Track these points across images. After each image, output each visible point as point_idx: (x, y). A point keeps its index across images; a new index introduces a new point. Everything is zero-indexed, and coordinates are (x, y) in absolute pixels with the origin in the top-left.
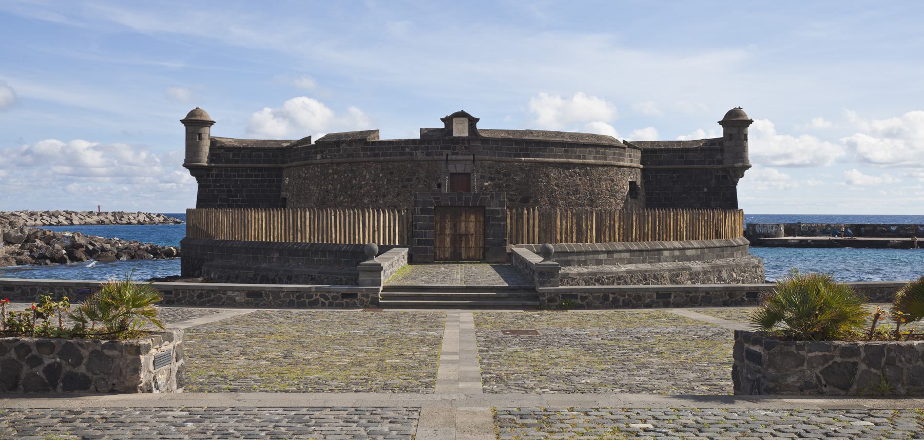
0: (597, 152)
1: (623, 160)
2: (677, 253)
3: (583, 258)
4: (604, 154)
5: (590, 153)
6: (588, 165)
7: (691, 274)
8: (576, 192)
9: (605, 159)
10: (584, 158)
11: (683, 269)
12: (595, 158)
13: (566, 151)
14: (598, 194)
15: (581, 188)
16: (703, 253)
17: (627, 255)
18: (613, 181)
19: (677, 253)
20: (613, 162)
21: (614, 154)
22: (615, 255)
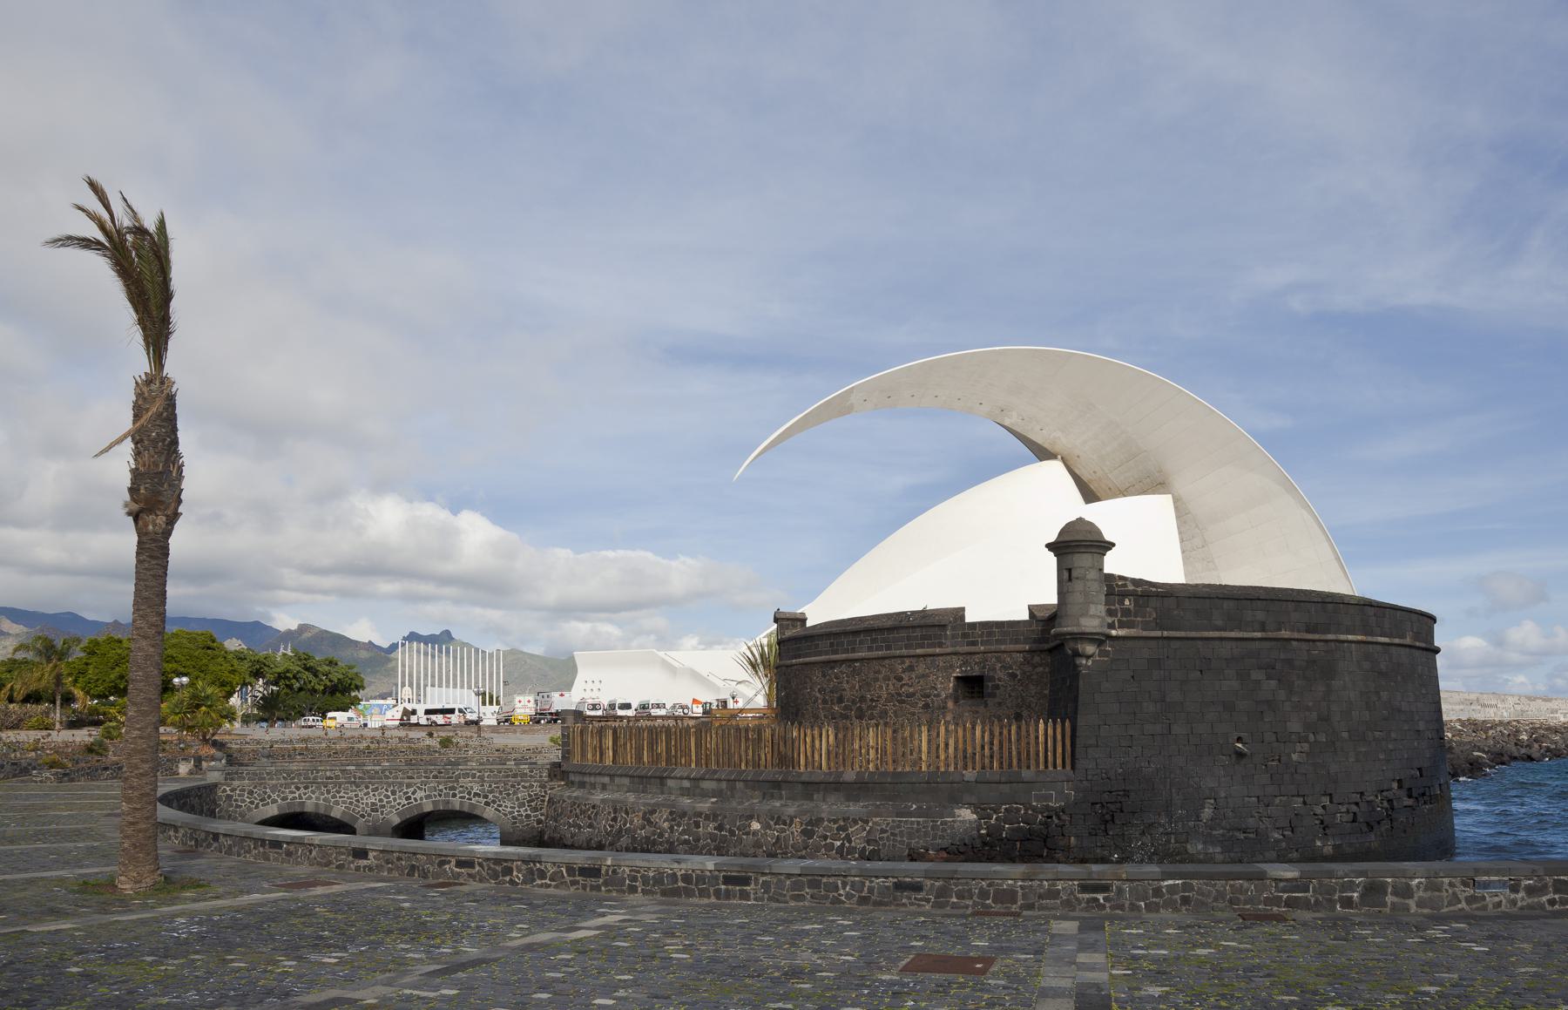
0: (874, 641)
1: (940, 645)
2: (686, 784)
3: (592, 779)
4: (884, 640)
5: (861, 642)
8: (840, 700)
9: (889, 648)
10: (853, 651)
12: (870, 649)
15: (847, 694)
16: (733, 789)
17: (626, 781)
18: (900, 679)
19: (686, 784)
20: (904, 652)
21: (909, 638)
22: (617, 780)
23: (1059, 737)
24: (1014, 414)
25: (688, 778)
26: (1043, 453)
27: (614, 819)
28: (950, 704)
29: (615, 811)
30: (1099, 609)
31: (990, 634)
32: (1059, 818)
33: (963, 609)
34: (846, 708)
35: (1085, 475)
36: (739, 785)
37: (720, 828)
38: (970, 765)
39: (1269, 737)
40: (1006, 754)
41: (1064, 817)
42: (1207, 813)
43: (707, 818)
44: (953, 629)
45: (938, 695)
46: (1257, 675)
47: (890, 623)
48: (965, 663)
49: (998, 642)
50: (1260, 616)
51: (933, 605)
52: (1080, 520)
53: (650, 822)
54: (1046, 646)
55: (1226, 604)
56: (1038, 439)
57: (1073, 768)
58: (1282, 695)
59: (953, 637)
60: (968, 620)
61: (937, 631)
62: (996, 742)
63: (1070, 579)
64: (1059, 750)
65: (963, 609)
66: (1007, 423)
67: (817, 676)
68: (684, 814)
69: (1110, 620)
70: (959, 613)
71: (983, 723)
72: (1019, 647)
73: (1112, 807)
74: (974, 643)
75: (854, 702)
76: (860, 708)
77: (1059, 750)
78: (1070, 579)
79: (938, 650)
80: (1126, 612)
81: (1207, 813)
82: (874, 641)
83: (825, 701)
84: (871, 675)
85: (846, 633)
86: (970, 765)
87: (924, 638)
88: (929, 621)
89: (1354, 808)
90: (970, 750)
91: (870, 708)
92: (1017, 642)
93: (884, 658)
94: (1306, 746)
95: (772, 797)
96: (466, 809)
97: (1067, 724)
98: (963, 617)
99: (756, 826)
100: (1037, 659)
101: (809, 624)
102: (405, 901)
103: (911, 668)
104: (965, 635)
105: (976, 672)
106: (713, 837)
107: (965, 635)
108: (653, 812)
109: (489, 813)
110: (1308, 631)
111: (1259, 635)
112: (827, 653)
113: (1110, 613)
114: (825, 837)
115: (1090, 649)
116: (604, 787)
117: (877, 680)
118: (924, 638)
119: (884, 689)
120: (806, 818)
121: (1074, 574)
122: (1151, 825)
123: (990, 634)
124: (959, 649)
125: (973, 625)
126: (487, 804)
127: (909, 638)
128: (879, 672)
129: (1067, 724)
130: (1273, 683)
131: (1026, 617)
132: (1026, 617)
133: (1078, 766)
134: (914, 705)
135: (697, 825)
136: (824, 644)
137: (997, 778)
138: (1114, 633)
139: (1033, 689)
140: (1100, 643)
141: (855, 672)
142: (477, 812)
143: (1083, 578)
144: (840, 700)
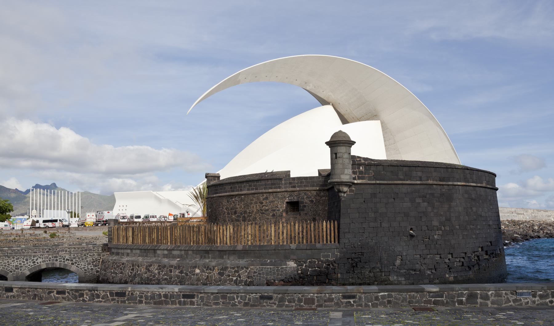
0: (250, 186)
1: (280, 188)
2: (166, 252)
3: (122, 251)
5: (244, 187)
6: (242, 195)
7: (159, 266)
8: (235, 213)
9: (257, 189)
10: (241, 190)
11: (156, 262)
12: (248, 190)
13: (231, 188)
14: (249, 213)
15: (239, 210)
16: (187, 254)
17: (138, 251)
18: (262, 203)
19: (166, 252)
20: (264, 191)
21: (265, 185)
22: (134, 251)
23: (332, 229)
24: (311, 85)
25: (167, 250)
26: (324, 102)
27: (133, 270)
28: (284, 214)
29: (133, 266)
30: (350, 171)
31: (301, 182)
32: (333, 265)
33: (289, 171)
34: (238, 216)
35: (342, 112)
36: (190, 252)
37: (181, 272)
38: (293, 242)
39: (425, 228)
40: (309, 237)
41: (335, 265)
42: (398, 262)
43: (175, 268)
44: (285, 180)
45: (279, 210)
46: (419, 200)
47: (257, 178)
48: (290, 196)
49: (305, 186)
50: (419, 174)
51: (275, 170)
52: (340, 131)
53: (149, 270)
54: (326, 188)
55: (405, 169)
56: (322, 96)
57: (339, 242)
58: (430, 209)
59: (285, 184)
60: (291, 176)
61: (278, 181)
62: (305, 231)
63: (336, 158)
64: (333, 235)
65: (289, 171)
66: (308, 88)
67: (225, 202)
68: (165, 266)
69: (354, 176)
70: (287, 173)
71: (299, 223)
72: (314, 188)
73: (356, 260)
74: (294, 187)
75: (241, 214)
76: (244, 217)
77: (333, 235)
78: (336, 158)
79: (278, 190)
80: (361, 172)
81: (398, 262)
82: (250, 186)
83: (228, 214)
84: (249, 201)
85: (237, 183)
86: (293, 242)
87: (272, 184)
88: (275, 177)
89: (462, 260)
90: (293, 235)
91: (248, 216)
92: (313, 186)
93: (254, 194)
94: (440, 232)
95: (205, 257)
96: (62, 267)
97: (336, 222)
98: (289, 175)
99: (197, 271)
100: (322, 194)
101: (221, 178)
102: (31, 311)
103: (267, 198)
104: (290, 183)
105: (295, 199)
106: (178, 277)
107: (290, 183)
108: (150, 266)
109: (73, 268)
110: (440, 181)
111: (419, 182)
112: (229, 192)
113: (354, 173)
114: (229, 276)
115: (345, 189)
116: (128, 255)
117: (251, 203)
118: (272, 184)
119: (255, 208)
120: (220, 267)
121: (338, 155)
122: (374, 268)
123: (301, 182)
124: (288, 189)
125: (294, 179)
126: (72, 264)
127: (265, 185)
128: (252, 200)
129: (336, 222)
130: (426, 204)
131: (317, 175)
132: (317, 175)
133: (341, 242)
134: (268, 215)
135: (171, 271)
136: (228, 188)
137: (305, 247)
138: (356, 182)
139: (320, 207)
140: (350, 186)
141: (242, 200)
142: (68, 268)
143: (342, 157)
144: (235, 213)
